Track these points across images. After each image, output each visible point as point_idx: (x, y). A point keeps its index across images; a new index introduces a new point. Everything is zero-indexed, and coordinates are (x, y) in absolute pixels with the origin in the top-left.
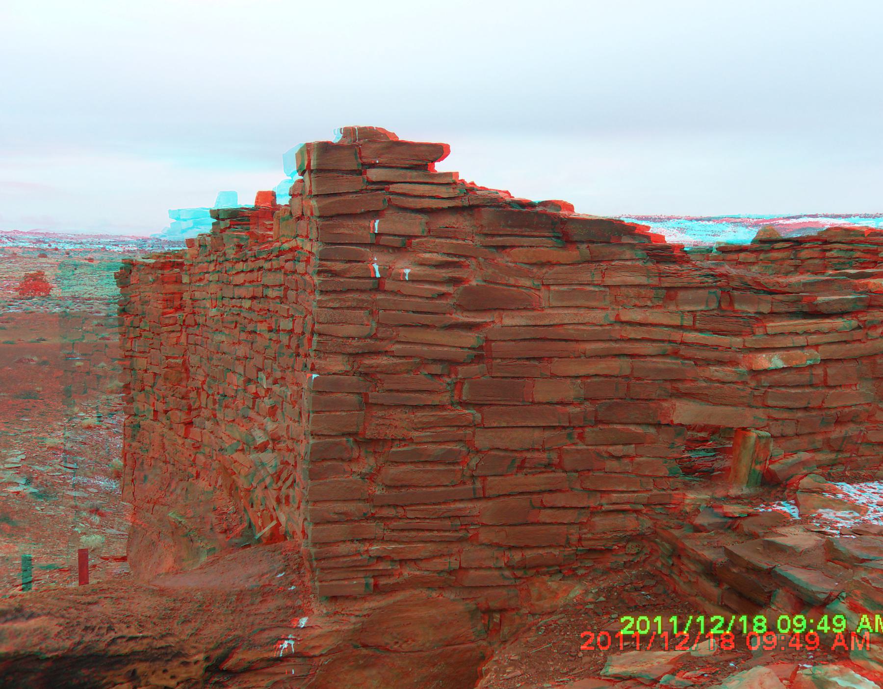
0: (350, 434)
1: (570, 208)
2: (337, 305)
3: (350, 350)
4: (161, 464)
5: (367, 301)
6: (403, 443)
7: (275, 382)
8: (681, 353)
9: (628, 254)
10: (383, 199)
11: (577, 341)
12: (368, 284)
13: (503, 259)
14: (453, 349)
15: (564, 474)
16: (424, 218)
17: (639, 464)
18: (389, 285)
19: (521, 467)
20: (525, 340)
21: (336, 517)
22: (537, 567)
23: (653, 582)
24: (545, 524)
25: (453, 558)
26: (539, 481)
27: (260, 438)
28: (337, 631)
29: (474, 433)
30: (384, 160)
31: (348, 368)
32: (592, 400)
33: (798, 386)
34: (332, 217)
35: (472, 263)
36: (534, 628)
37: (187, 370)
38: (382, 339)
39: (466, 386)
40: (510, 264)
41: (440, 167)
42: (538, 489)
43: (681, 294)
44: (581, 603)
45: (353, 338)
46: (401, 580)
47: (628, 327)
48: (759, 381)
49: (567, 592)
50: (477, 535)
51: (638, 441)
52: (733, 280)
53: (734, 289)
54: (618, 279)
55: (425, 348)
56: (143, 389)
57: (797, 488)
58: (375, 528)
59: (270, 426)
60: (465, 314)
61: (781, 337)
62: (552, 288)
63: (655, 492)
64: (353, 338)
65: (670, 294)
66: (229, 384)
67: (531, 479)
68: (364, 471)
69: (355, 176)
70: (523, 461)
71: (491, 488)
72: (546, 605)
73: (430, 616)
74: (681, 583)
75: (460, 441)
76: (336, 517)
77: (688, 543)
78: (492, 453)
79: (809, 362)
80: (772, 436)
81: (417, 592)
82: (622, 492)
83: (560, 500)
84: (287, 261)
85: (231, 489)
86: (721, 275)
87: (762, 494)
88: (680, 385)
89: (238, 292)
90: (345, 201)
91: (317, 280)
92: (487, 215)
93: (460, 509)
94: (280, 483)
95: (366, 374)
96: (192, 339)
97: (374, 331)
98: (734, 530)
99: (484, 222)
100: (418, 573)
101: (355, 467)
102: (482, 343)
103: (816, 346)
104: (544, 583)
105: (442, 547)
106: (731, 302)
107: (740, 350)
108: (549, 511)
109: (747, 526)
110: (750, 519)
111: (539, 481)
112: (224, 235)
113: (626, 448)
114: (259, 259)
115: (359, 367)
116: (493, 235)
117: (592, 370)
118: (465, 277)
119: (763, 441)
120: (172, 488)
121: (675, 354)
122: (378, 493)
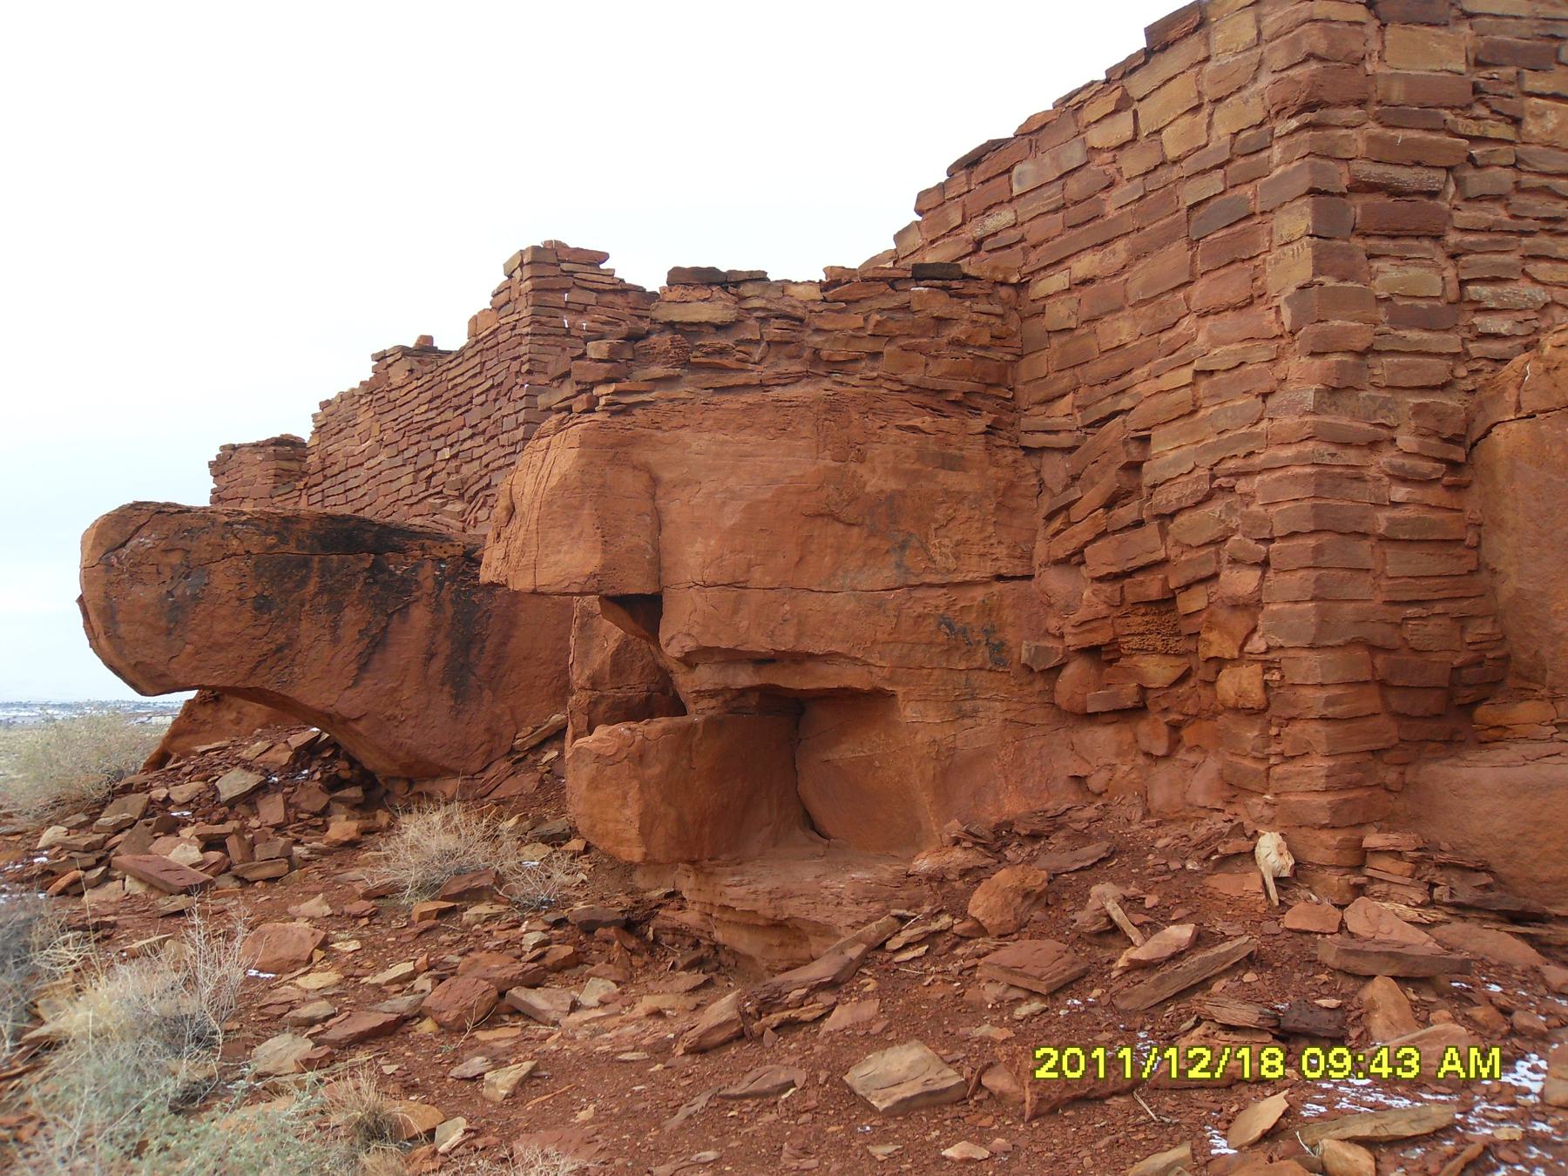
18: (573, 332)
41: (602, 266)
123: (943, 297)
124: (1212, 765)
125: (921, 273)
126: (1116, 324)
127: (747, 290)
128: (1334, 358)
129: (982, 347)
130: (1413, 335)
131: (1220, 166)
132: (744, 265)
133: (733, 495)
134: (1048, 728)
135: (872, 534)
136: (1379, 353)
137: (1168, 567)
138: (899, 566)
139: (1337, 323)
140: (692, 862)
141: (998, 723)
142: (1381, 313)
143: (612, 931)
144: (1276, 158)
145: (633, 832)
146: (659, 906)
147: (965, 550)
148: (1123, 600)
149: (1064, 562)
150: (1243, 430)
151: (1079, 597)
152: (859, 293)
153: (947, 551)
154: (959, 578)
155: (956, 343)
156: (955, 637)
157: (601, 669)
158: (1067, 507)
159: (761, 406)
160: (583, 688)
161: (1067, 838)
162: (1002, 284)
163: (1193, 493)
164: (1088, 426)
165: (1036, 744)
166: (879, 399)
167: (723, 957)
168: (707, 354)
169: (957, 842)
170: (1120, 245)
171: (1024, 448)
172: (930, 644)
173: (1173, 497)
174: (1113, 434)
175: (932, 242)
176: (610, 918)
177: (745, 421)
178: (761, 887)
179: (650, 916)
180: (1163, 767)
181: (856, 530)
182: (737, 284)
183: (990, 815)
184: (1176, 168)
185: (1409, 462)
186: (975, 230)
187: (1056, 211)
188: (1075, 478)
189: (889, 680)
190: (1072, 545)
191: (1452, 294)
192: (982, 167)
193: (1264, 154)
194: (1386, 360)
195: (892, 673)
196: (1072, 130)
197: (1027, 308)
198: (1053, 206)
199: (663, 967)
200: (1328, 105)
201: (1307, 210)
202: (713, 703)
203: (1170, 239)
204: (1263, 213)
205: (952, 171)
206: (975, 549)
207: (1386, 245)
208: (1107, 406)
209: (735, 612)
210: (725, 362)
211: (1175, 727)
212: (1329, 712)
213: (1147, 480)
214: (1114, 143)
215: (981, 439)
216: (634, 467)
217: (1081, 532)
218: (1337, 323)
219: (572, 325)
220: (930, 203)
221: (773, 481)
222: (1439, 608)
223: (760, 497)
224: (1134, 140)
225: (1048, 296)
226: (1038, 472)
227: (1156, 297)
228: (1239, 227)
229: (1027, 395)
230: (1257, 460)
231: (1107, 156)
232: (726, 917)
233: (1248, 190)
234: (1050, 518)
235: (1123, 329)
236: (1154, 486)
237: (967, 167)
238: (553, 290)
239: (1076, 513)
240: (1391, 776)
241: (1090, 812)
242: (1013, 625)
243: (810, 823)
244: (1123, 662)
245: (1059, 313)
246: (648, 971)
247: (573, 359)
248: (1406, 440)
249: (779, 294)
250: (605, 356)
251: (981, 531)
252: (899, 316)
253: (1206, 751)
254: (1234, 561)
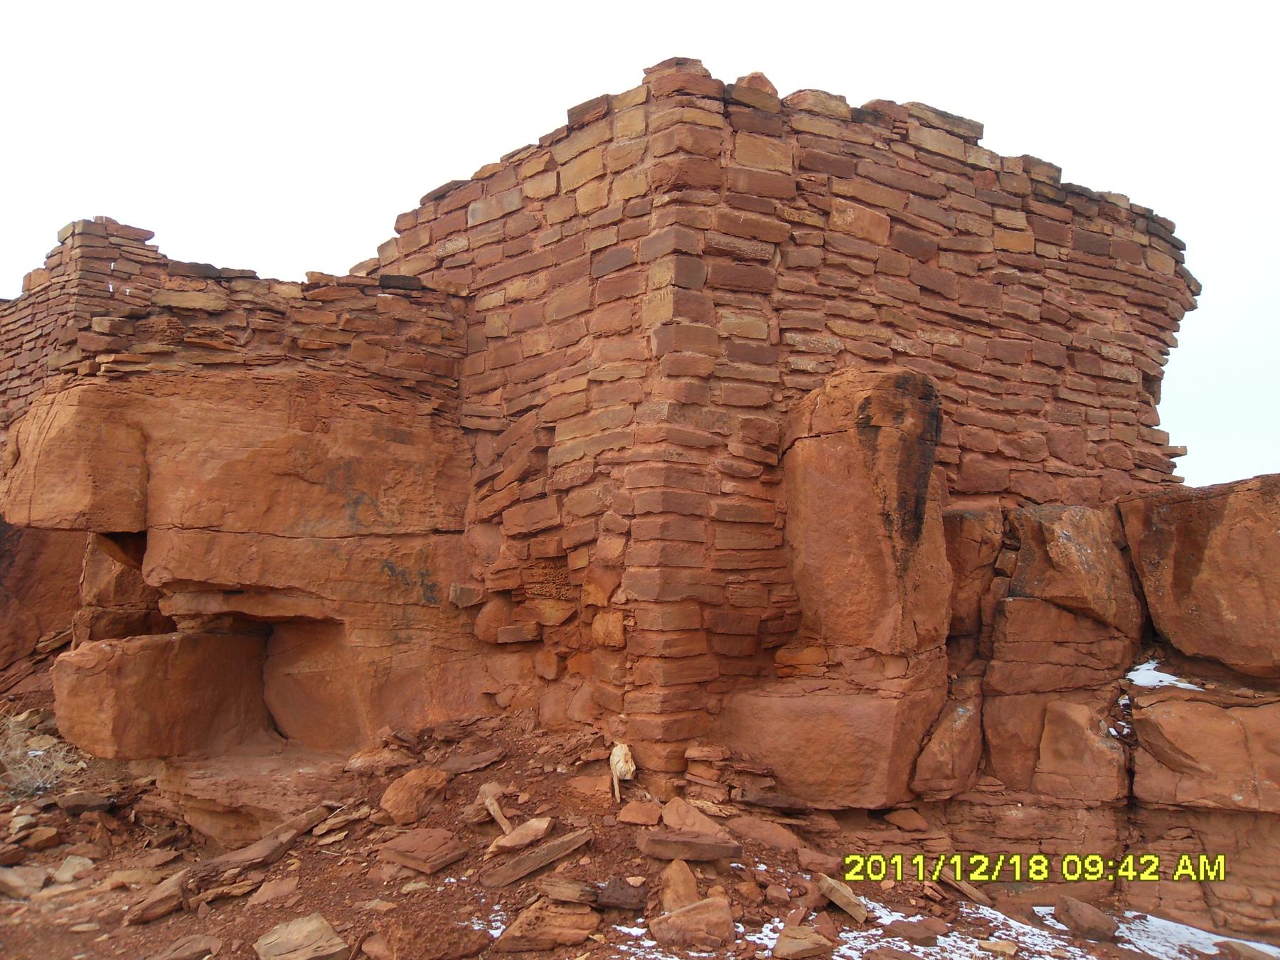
12: (108, 295)
41: (147, 243)
123: (404, 303)
124: (587, 689)
125: (387, 283)
126: (536, 337)
127: (238, 285)
128: (684, 381)
129: (433, 345)
130: (745, 366)
131: (615, 224)
132: (237, 264)
133: (214, 455)
134: (469, 654)
135: (331, 492)
136: (719, 378)
137: (562, 532)
138: (352, 518)
139: (688, 354)
140: (164, 758)
141: (427, 649)
142: (723, 349)
143: (95, 815)
144: (653, 224)
145: (106, 733)
146: (144, 792)
147: (408, 508)
148: (529, 555)
149: (486, 521)
150: (619, 430)
151: (495, 549)
152: (334, 295)
153: (393, 508)
154: (402, 531)
155: (412, 340)
156: (396, 578)
157: (107, 588)
158: (492, 478)
159: (242, 381)
160: (90, 605)
161: (473, 744)
162: (455, 296)
163: (582, 475)
164: (512, 415)
165: (459, 666)
166: (345, 382)
167: (195, 836)
168: (200, 335)
169: (386, 744)
170: (542, 275)
171: (464, 428)
172: (374, 583)
173: (568, 477)
174: (529, 423)
175: (406, 256)
176: (95, 803)
177: (228, 393)
178: (220, 779)
179: (136, 799)
180: (553, 687)
181: (317, 488)
182: (229, 280)
183: (416, 723)
184: (585, 221)
185: (736, 463)
186: (438, 251)
187: (498, 242)
188: (500, 456)
189: (339, 611)
190: (494, 509)
191: (775, 339)
192: (446, 201)
193: (646, 219)
194: (724, 384)
195: (342, 605)
196: (513, 181)
197: (472, 317)
198: (496, 239)
199: (140, 845)
200: (691, 187)
201: (672, 265)
202: (192, 623)
203: (579, 275)
204: (642, 263)
205: (424, 201)
206: (417, 507)
207: (729, 296)
208: (526, 401)
209: (208, 551)
210: (214, 343)
211: (562, 658)
212: (667, 652)
213: (551, 462)
214: (543, 195)
215: (428, 420)
216: (128, 425)
217: (500, 499)
218: (688, 354)
219: (116, 290)
220: (407, 224)
221: (249, 445)
222: (753, 576)
223: (237, 457)
224: (556, 195)
225: (488, 310)
226: (473, 448)
227: (566, 319)
228: (625, 272)
229: (469, 386)
230: (627, 454)
231: (537, 205)
232: (190, 804)
233: (633, 245)
234: (479, 485)
235: (540, 342)
236: (556, 467)
237: (436, 199)
239: (499, 483)
240: (712, 702)
241: (495, 723)
242: (444, 570)
243: (273, 725)
244: (527, 604)
245: (496, 323)
246: (124, 849)
247: (80, 330)
248: (735, 447)
249: (266, 291)
250: (107, 330)
251: (423, 492)
252: (366, 316)
253: (583, 678)
254: (607, 530)
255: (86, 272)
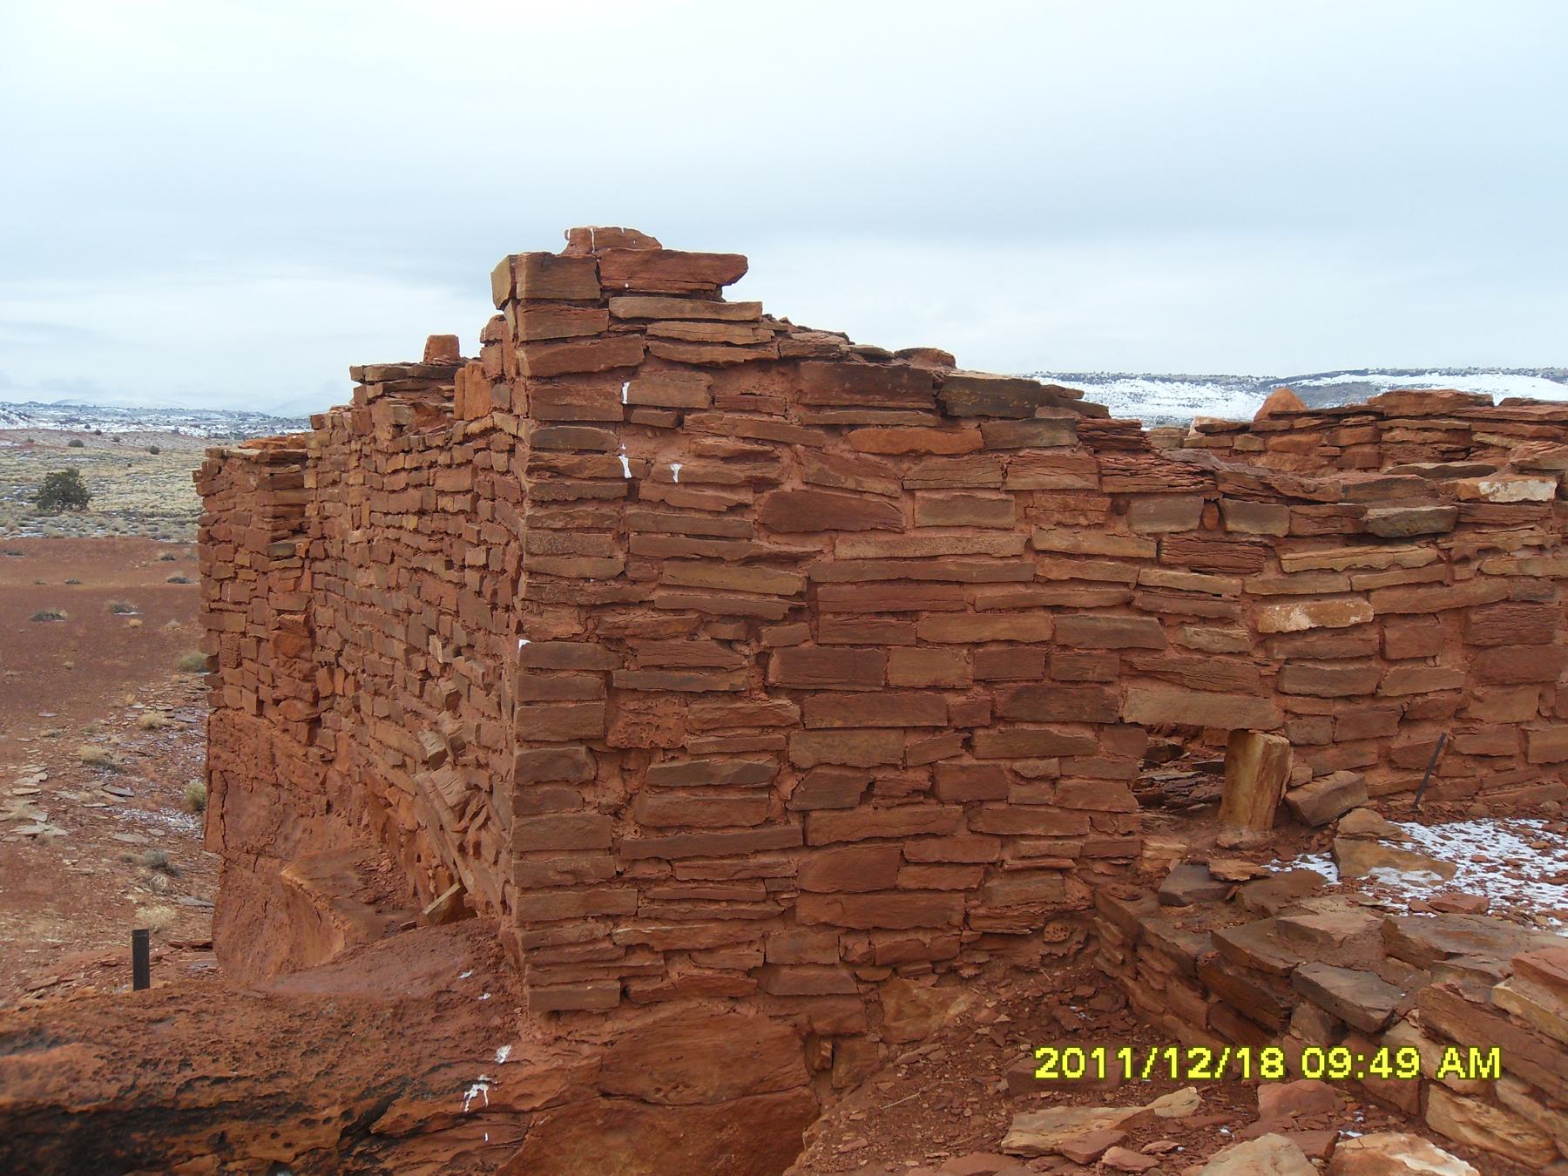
0: (581, 740)
1: (949, 361)
2: (559, 525)
3: (582, 600)
4: (271, 789)
5: (610, 517)
6: (670, 755)
7: (458, 653)
8: (1137, 603)
9: (1047, 436)
10: (635, 343)
11: (960, 583)
13: (838, 448)
14: (753, 598)
15: (939, 808)
16: (705, 379)
17: (1066, 791)
18: (646, 490)
19: (866, 796)
20: (873, 582)
21: (558, 877)
22: (895, 966)
23: (1090, 991)
24: (907, 891)
25: (755, 947)
26: (899, 819)
27: (433, 746)
28: (559, 1069)
29: (788, 738)
30: (638, 282)
31: (578, 629)
32: (988, 683)
33: (1336, 660)
34: (550, 379)
35: (785, 454)
36: (890, 1065)
37: (312, 633)
38: (635, 582)
39: (774, 662)
40: (847, 455)
41: (732, 294)
42: (896, 832)
43: (1136, 504)
44: (967, 1025)
45: (587, 579)
46: (665, 984)
47: (1048, 561)
48: (1268, 651)
49: (944, 1005)
50: (793, 908)
51: (1066, 752)
52: (1225, 480)
53: (1225, 495)
54: (1030, 480)
55: (706, 596)
56: (239, 665)
57: (1335, 832)
58: (625, 898)
59: (449, 725)
60: (773, 538)
61: (1307, 577)
62: (918, 494)
63: (1093, 837)
64: (587, 579)
65: (1119, 506)
66: (381, 655)
67: (883, 815)
68: (604, 801)
69: (590, 310)
70: (871, 785)
71: (816, 831)
72: (909, 1028)
73: (717, 1046)
74: (1138, 992)
75: (765, 751)
76: (558, 877)
77: (1150, 925)
78: (819, 770)
79: (1354, 619)
80: (1292, 744)
81: (693, 1004)
82: (1039, 837)
83: (932, 850)
84: (477, 451)
85: (384, 830)
86: (1203, 473)
87: (1276, 843)
88: (1137, 659)
89: (395, 503)
90: (571, 351)
91: (527, 483)
92: (810, 375)
93: (764, 866)
94: (464, 823)
95: (606, 639)
96: (321, 581)
97: (621, 568)
98: (1228, 902)
99: (804, 386)
100: (695, 972)
101: (589, 795)
102: (798, 585)
103: (1366, 593)
104: (907, 990)
105: (734, 929)
106: (1221, 519)
107: (1236, 599)
108: (912, 869)
109: (1250, 896)
110: (1256, 884)
111: (899, 819)
112: (374, 409)
113: (1042, 763)
114: (430, 448)
115: (596, 627)
116: (819, 407)
117: (986, 634)
118: (773, 476)
119: (1276, 753)
120: (286, 829)
121: (1127, 604)
122: (628, 838)
219: (644, 468)
238: (587, 375)
255: (553, 420)
